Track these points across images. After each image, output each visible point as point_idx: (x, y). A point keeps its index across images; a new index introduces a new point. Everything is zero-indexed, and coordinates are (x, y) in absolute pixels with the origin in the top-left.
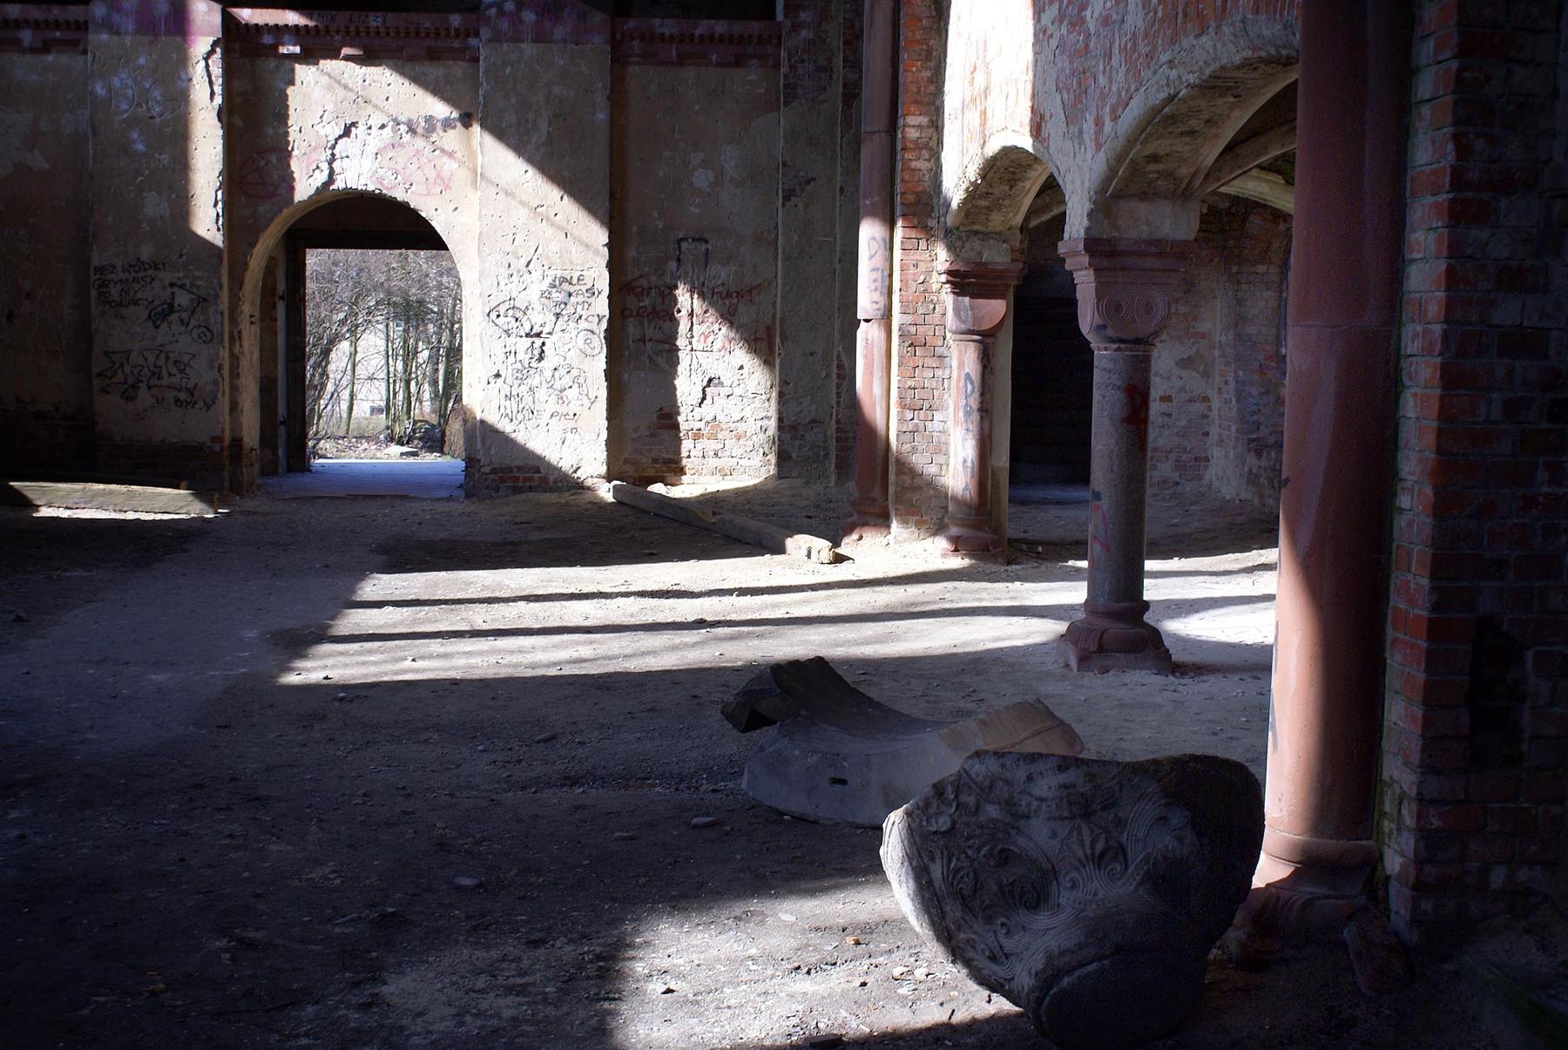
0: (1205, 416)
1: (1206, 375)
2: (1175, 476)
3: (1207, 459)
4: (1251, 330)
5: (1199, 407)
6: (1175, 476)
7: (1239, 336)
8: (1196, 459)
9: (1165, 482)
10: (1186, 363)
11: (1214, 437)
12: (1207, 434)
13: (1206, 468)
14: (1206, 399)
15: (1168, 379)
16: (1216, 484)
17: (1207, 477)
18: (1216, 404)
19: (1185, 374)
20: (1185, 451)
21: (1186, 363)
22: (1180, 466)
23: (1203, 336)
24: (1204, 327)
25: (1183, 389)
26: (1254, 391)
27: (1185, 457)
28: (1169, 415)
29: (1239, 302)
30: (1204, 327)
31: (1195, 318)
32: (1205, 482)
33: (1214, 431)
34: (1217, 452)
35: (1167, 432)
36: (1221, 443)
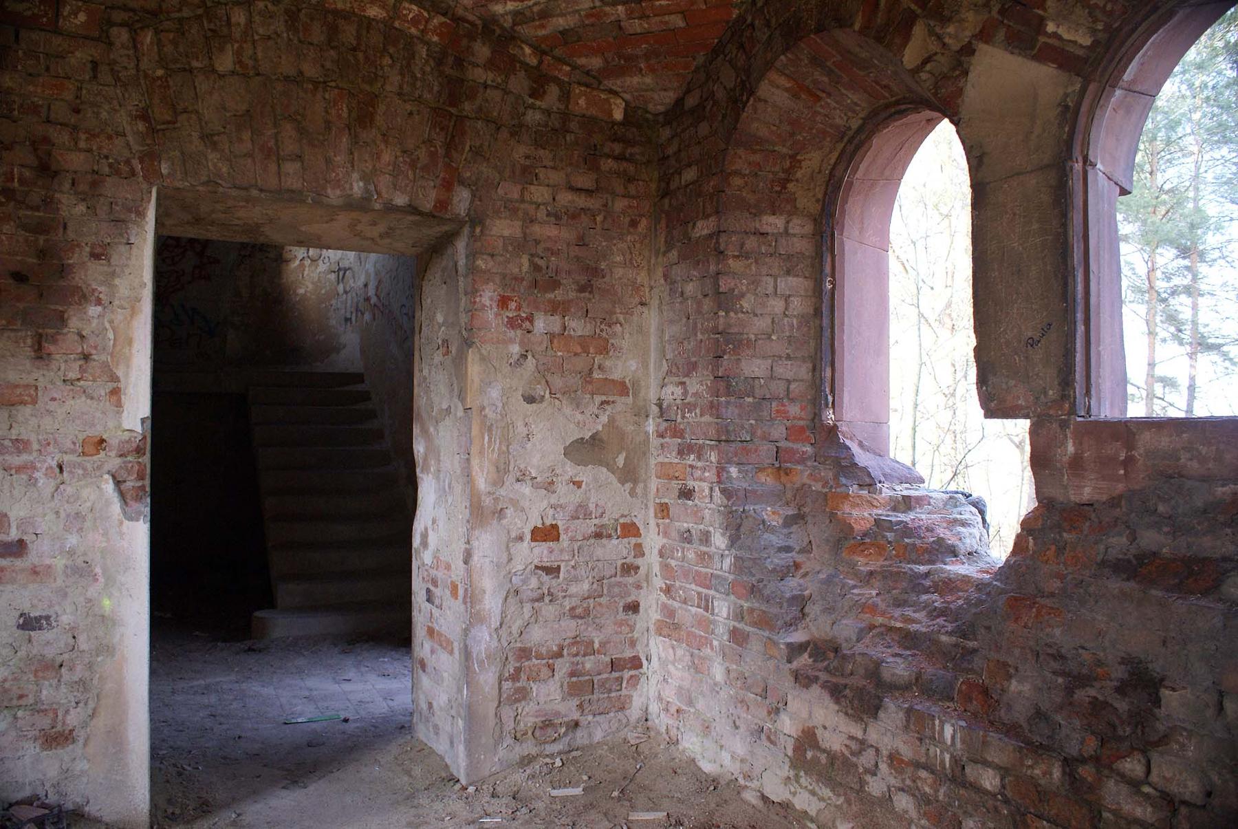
0: (629, 569)
1: (629, 475)
2: (569, 709)
3: (636, 663)
4: (754, 367)
5: (616, 549)
6: (569, 709)
7: (724, 384)
8: (614, 665)
9: (547, 724)
10: (587, 449)
11: (651, 612)
12: (634, 608)
13: (634, 681)
14: (630, 530)
15: (549, 486)
16: (662, 721)
17: (637, 702)
18: (652, 540)
19: (586, 474)
20: (590, 650)
21: (587, 449)
22: (579, 686)
23: (622, 388)
24: (623, 367)
25: (582, 512)
26: (771, 514)
27: (589, 663)
28: (553, 571)
29: (724, 300)
30: (623, 367)
31: (604, 350)
32: (634, 713)
33: (652, 603)
34: (657, 649)
35: (548, 610)
36: (670, 627)
